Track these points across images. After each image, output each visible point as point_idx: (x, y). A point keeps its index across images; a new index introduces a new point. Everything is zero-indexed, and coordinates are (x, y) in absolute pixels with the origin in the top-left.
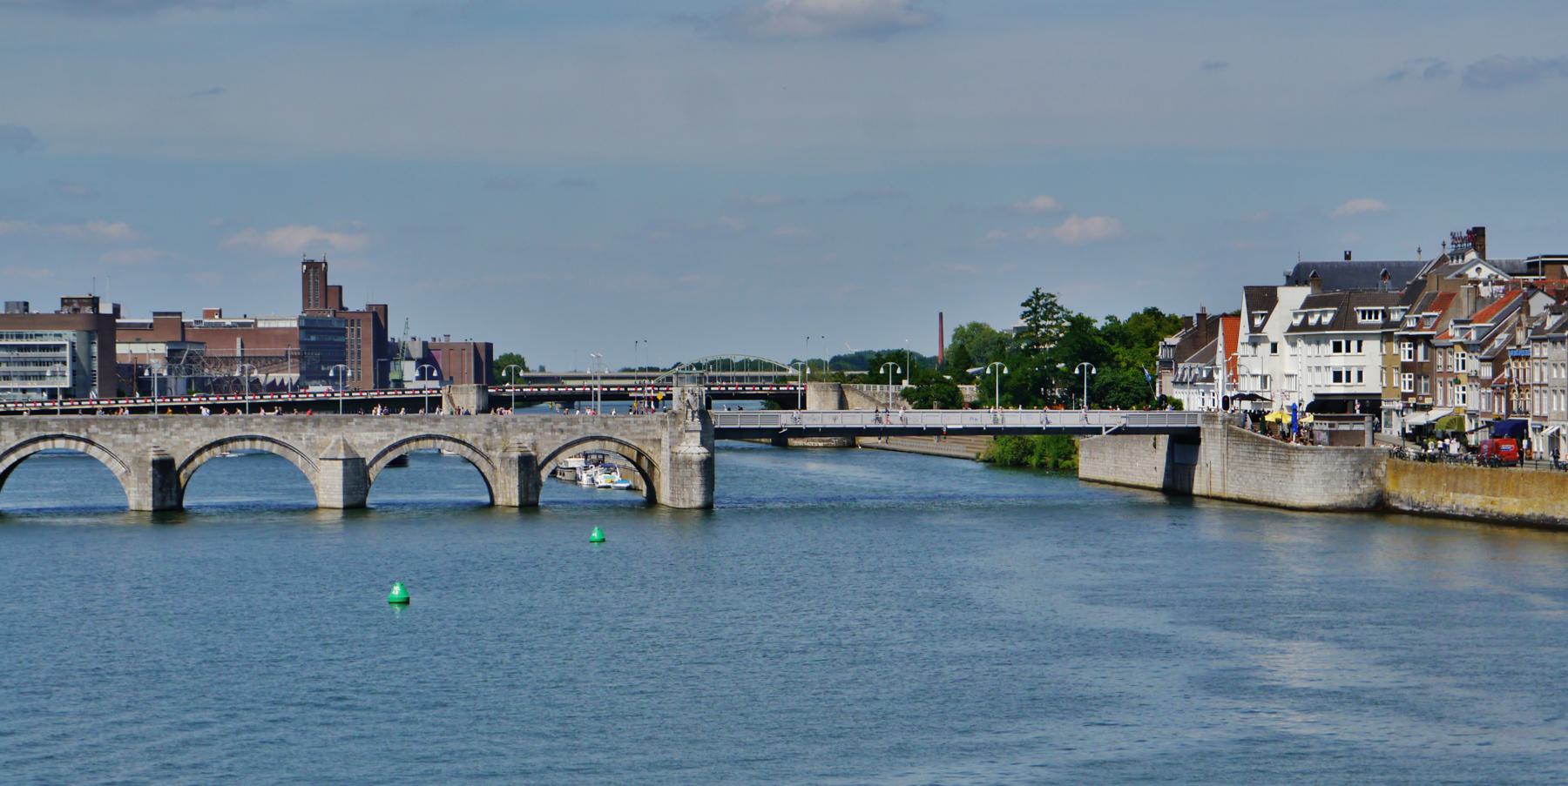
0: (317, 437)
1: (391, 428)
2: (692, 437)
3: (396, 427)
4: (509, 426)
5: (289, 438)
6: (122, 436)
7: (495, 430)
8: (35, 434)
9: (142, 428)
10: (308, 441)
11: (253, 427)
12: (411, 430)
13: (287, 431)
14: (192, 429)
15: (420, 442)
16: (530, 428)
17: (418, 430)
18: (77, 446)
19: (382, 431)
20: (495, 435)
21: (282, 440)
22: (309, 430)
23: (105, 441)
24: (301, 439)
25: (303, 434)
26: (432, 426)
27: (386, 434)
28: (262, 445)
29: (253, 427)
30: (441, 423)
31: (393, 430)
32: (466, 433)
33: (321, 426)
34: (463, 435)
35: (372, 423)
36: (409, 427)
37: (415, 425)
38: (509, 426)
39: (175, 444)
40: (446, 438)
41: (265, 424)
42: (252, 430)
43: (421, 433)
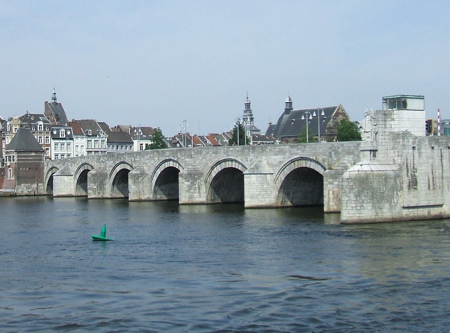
0: (254, 159)
1: (284, 154)
2: (364, 156)
3: (286, 152)
4: (340, 150)
5: (243, 160)
6: (187, 159)
7: (333, 153)
8: (163, 159)
9: (193, 155)
10: (251, 162)
11: (230, 153)
12: (293, 154)
13: (243, 156)
14: (209, 155)
15: (296, 162)
16: (351, 151)
17: (297, 154)
18: (173, 165)
19: (280, 155)
20: (333, 157)
21: (241, 161)
22: (251, 155)
23: (182, 163)
24: (247, 161)
25: (249, 157)
26: (303, 151)
27: (282, 157)
28: (235, 165)
29: (230, 153)
30: (307, 149)
31: (284, 154)
32: (319, 156)
33: (256, 152)
34: (318, 157)
35: (276, 150)
36: (292, 152)
37: (294, 150)
38: (340, 150)
39: (204, 164)
40: (311, 160)
41: (234, 151)
42: (229, 155)
43: (298, 156)
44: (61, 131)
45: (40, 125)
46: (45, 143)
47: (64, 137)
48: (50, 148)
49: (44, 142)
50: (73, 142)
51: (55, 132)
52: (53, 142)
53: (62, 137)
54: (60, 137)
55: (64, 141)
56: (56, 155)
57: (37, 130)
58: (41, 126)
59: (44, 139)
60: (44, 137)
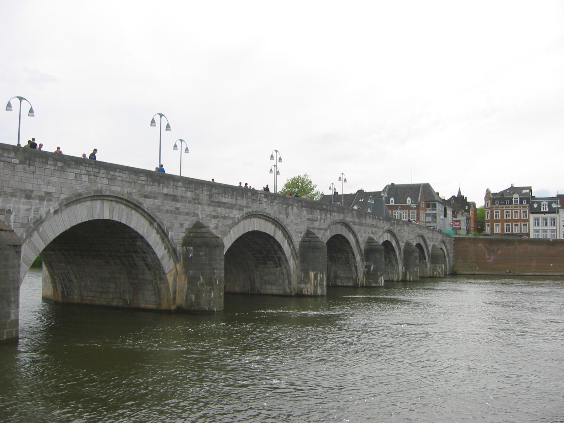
44: (542, 204)
45: (515, 198)
46: (522, 218)
47: (547, 210)
48: (528, 223)
49: (520, 217)
50: (558, 216)
51: (535, 206)
52: (532, 217)
53: (544, 211)
54: (542, 210)
55: (547, 215)
56: (537, 231)
57: (512, 204)
58: (516, 200)
59: (520, 214)
60: (520, 211)
